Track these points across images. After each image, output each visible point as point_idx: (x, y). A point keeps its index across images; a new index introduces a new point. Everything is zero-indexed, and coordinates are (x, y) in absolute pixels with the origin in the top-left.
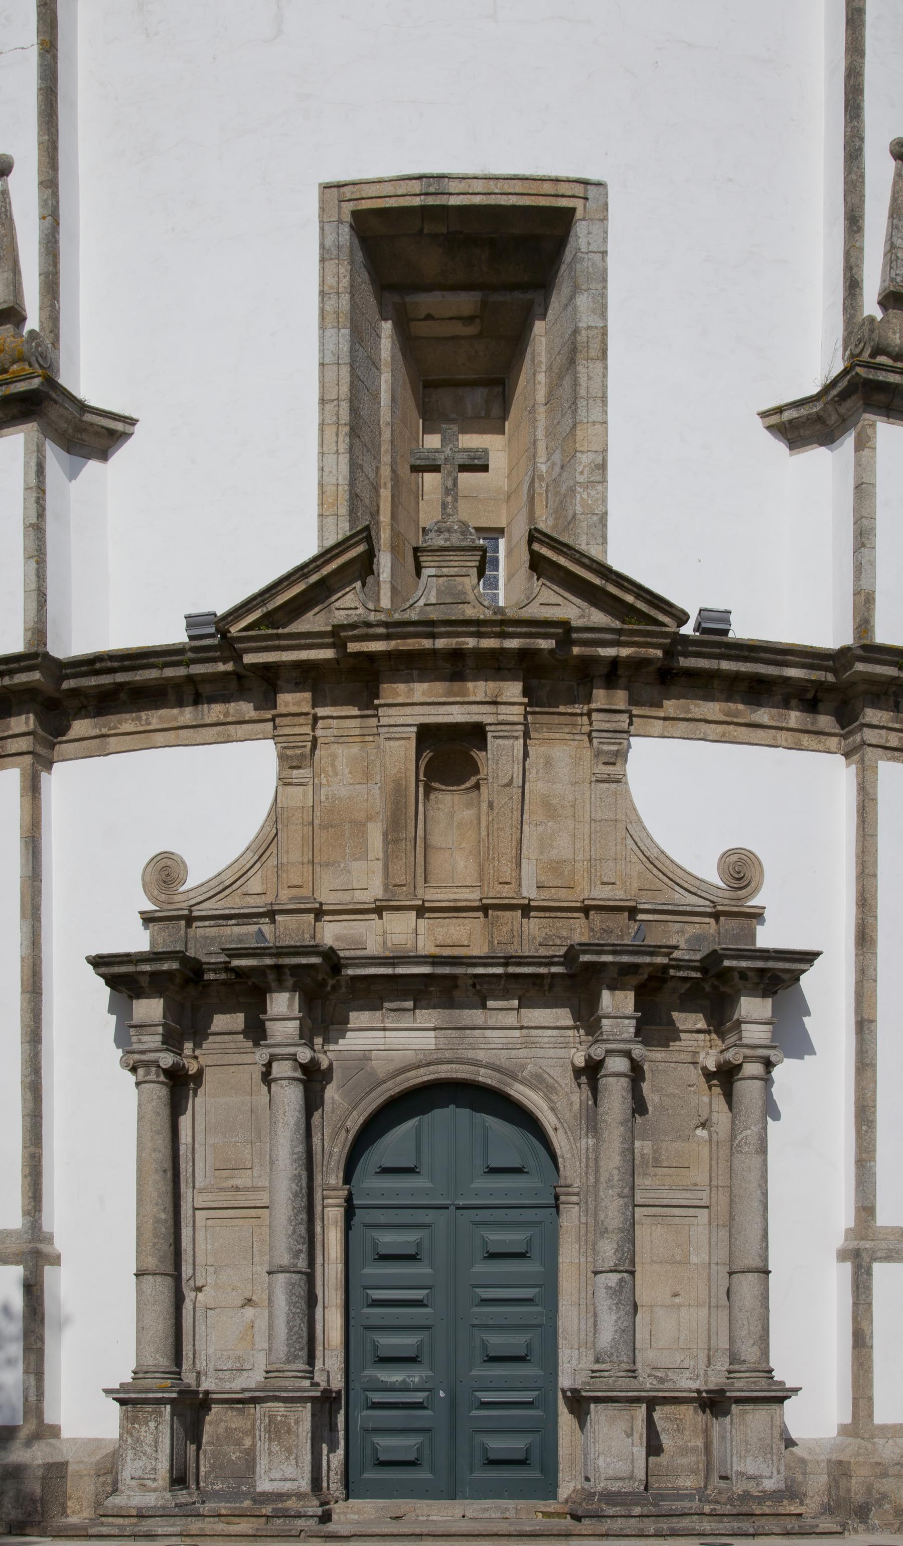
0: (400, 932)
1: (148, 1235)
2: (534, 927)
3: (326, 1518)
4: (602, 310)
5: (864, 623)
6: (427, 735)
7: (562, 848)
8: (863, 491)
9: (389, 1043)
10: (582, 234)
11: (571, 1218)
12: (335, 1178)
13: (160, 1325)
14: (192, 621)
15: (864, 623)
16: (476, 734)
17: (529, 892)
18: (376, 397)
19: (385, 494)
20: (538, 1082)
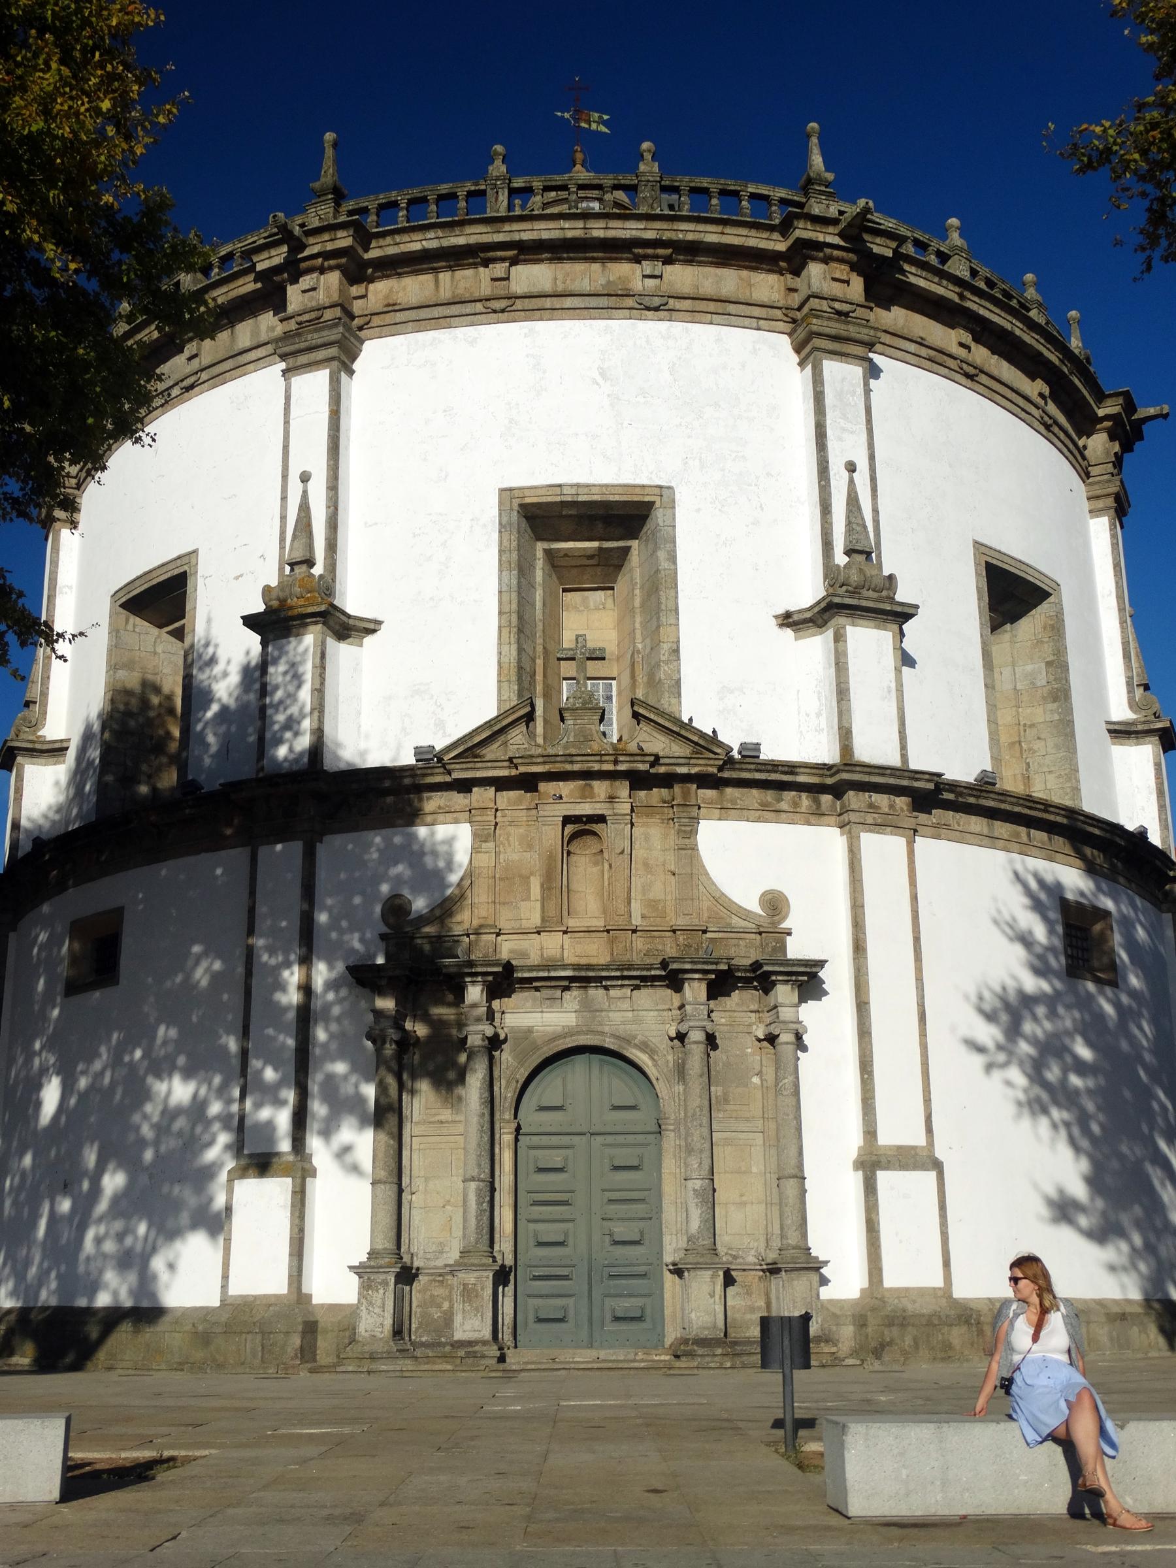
0: (552, 945)
1: (381, 1155)
2: (639, 943)
3: (502, 1359)
4: (673, 559)
5: (846, 747)
6: (567, 820)
7: (657, 892)
8: (841, 665)
11: (670, 1140)
12: (508, 1115)
13: (388, 1220)
14: (418, 751)
15: (846, 747)
16: (601, 819)
17: (637, 921)
18: (533, 605)
19: (539, 662)
20: (645, 1047)
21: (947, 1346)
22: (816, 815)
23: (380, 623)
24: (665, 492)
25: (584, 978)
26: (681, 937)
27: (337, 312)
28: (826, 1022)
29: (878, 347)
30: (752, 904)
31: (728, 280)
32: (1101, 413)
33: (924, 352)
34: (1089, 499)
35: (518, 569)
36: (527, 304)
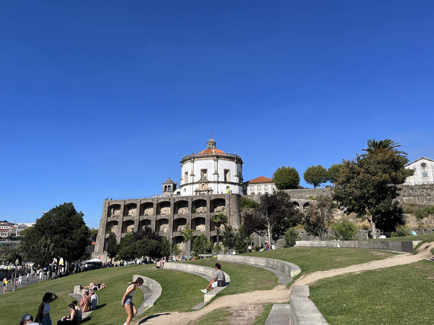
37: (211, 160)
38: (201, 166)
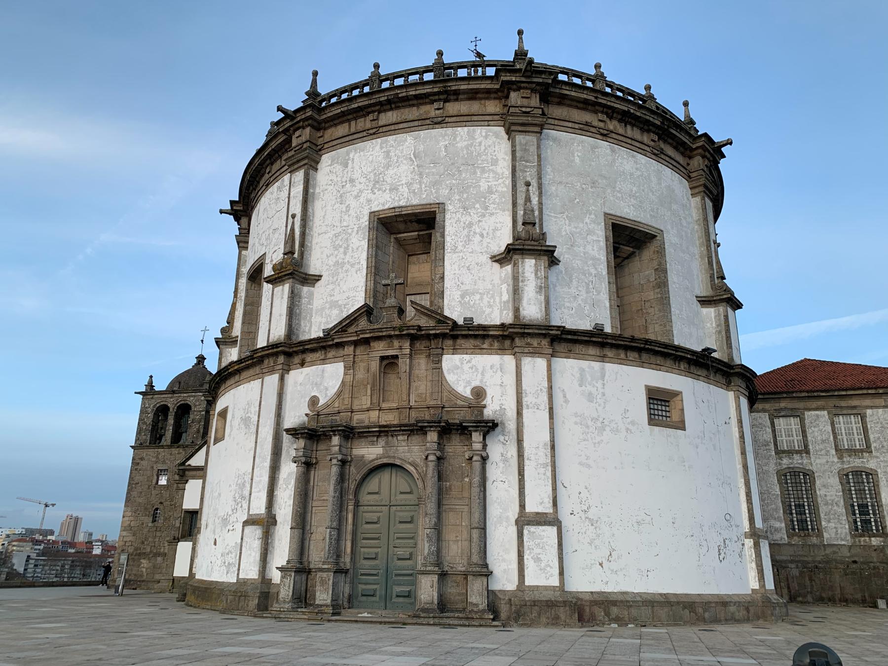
6: (383, 358)
9: (370, 452)
10: (438, 218)
16: (396, 357)
17: (412, 403)
21: (557, 618)
22: (502, 351)
23: (321, 276)
24: (441, 205)
25: (384, 431)
26: (432, 411)
27: (308, 144)
28: (500, 451)
29: (546, 126)
30: (467, 393)
31: (475, 107)
32: (694, 146)
33: (577, 126)
34: (691, 188)
35: (376, 249)
36: (385, 129)
37: (480, 132)
38: (377, 183)
